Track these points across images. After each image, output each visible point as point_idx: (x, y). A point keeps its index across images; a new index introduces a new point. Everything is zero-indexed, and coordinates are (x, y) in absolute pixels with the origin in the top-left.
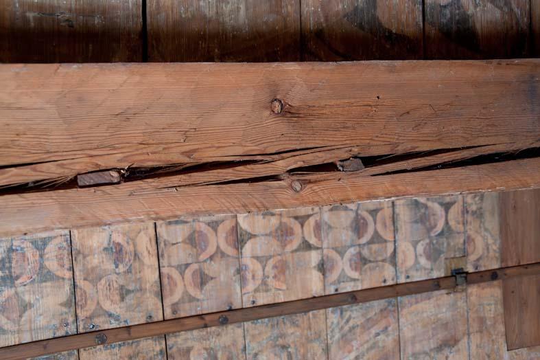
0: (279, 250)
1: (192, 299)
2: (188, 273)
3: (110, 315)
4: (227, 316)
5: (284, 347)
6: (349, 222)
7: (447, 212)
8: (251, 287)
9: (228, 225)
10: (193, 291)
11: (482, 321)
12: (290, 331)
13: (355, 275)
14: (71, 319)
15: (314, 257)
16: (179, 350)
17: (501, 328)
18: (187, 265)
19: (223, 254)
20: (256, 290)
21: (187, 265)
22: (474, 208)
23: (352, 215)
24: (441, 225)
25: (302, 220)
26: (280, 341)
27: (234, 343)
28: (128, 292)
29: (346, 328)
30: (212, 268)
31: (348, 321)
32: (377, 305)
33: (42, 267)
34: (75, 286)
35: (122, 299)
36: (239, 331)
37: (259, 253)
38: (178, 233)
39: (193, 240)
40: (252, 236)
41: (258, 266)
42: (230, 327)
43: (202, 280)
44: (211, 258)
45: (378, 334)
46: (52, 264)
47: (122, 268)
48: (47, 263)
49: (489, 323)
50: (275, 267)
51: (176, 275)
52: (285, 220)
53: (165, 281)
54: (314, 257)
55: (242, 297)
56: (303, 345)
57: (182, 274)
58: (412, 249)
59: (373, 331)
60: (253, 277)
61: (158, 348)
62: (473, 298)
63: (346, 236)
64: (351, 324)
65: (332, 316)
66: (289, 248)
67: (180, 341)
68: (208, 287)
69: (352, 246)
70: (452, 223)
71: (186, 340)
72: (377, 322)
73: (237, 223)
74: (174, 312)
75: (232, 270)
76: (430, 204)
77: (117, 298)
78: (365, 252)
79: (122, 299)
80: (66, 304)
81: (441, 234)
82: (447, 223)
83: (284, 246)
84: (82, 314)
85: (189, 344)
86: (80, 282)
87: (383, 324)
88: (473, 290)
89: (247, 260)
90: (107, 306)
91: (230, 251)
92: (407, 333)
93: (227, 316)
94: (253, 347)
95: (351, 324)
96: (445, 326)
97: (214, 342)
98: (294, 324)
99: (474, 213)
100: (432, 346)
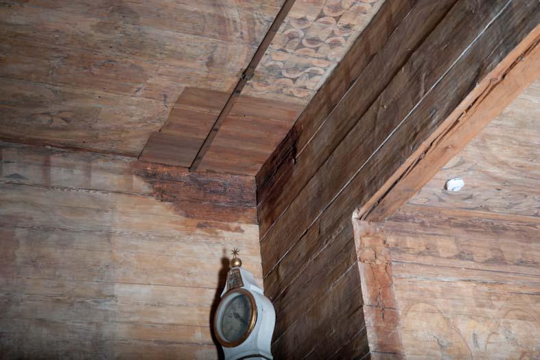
0: (328, 4)
6: (320, 37)
7: (292, 79)
13: (286, 33)
15: (311, 18)
22: (285, 90)
23: (323, 40)
24: (285, 74)
25: (337, 19)
31: (261, 23)
32: (260, 38)
45: (242, 33)
52: (344, 11)
54: (311, 18)
58: (282, 60)
59: (245, 33)
63: (312, 34)
64: (258, 24)
69: (305, 36)
70: (283, 79)
76: (302, 73)
78: (296, 40)
81: (281, 74)
82: (285, 77)
88: (236, 80)
95: (258, 24)
99: (281, 90)
100: (215, 56)
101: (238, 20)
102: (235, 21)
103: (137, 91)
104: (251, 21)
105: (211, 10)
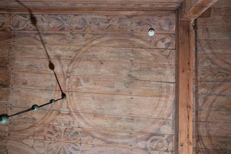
4: (196, 72)
5: (203, 62)
11: (204, 22)
12: (200, 60)
16: (200, 79)
17: (206, 18)
26: (202, 62)
27: (201, 70)
29: (201, 50)
32: (198, 44)
42: (198, 71)
49: (204, 21)
56: (203, 58)
59: (202, 45)
62: (199, 24)
65: (199, 52)
67: (199, 79)
72: (201, 44)
87: (201, 43)
88: (198, 24)
92: (204, 38)
93: (196, 72)
94: (202, 67)
96: (204, 30)
98: (199, 60)
101: (206, 49)
102: (207, 48)
103: (224, 11)
104: (203, 51)
105: (214, 51)
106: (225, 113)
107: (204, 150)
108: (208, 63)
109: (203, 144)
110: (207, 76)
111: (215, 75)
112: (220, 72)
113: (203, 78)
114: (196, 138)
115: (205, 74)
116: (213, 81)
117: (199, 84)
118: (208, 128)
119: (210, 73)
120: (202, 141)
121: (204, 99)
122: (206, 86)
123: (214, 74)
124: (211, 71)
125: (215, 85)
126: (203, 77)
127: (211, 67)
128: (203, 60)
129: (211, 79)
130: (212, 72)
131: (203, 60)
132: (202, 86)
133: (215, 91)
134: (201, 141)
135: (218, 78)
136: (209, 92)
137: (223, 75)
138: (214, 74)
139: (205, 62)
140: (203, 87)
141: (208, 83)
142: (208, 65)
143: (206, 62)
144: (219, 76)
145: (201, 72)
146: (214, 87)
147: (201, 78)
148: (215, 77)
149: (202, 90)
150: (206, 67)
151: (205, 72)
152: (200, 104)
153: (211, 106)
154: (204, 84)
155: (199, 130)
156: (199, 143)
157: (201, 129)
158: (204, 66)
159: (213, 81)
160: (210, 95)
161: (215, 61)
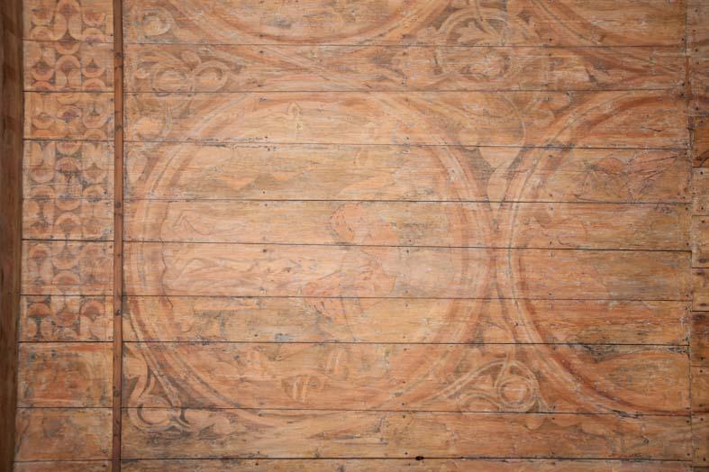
1: (105, 74)
2: (87, 75)
3: (107, 123)
4: (119, 54)
5: (144, 18)
8: (101, 37)
9: (58, 47)
10: (100, 73)
12: (133, 12)
14: (106, 144)
16: (136, 85)
18: (82, 75)
19: (78, 52)
20: (104, 33)
21: (82, 75)
26: (140, 20)
27: (137, 50)
28: (94, 111)
30: (86, 59)
33: (73, 156)
34: (86, 140)
35: (98, 115)
36: (130, 46)
37: (79, 29)
38: (61, 79)
39: (67, 70)
40: (67, 32)
41: (88, 30)
42: (126, 52)
43: (93, 66)
44: (79, 60)
46: (72, 151)
47: (80, 114)
48: (71, 153)
50: (90, 19)
51: (87, 83)
52: (58, 9)
53: (90, 89)
55: (107, 41)
56: (144, 5)
57: (88, 79)
60: (95, 34)
61: (132, 97)
66: (78, 9)
68: (97, 63)
71: (130, 80)
73: (58, 41)
74: (111, 85)
75: (89, 47)
77: (97, 118)
79: (98, 115)
80: (96, 145)
83: (77, 12)
84: (104, 138)
85: (133, 78)
86: (85, 137)
89: (83, 37)
90: (101, 123)
91: (76, 47)
93: (119, 54)
94: (141, 38)
97: (134, 64)
98: (129, 10)
106: (222, 207)
107: (144, 346)
108: (164, 22)
109: (142, 325)
110: (160, 74)
111: (192, 66)
112: (209, 59)
113: (146, 79)
114: (113, 302)
115: (155, 63)
116: (181, 92)
117: (130, 102)
118: (161, 267)
119: (173, 60)
120: (137, 312)
121: (149, 158)
122: (157, 109)
123: (187, 65)
124: (175, 54)
125: (189, 104)
126: (144, 75)
127: (175, 38)
128: (147, 13)
129: (177, 82)
130: (180, 58)
131: (147, 13)
132: (142, 110)
133: (188, 129)
134: (132, 316)
135: (201, 78)
136: (165, 134)
137: (220, 72)
138: (187, 65)
139: (150, 18)
140: (147, 115)
141: (163, 98)
142: (166, 30)
143: (158, 19)
144: (203, 71)
145: (139, 57)
146: (185, 114)
147: (137, 79)
148: (191, 78)
149: (139, 126)
150: (155, 39)
151: (154, 59)
152: (133, 177)
153: (173, 184)
154: (149, 102)
155: (126, 275)
156: (126, 324)
157: (134, 268)
158: (149, 33)
159: (181, 92)
160: (172, 141)
161: (190, 15)
